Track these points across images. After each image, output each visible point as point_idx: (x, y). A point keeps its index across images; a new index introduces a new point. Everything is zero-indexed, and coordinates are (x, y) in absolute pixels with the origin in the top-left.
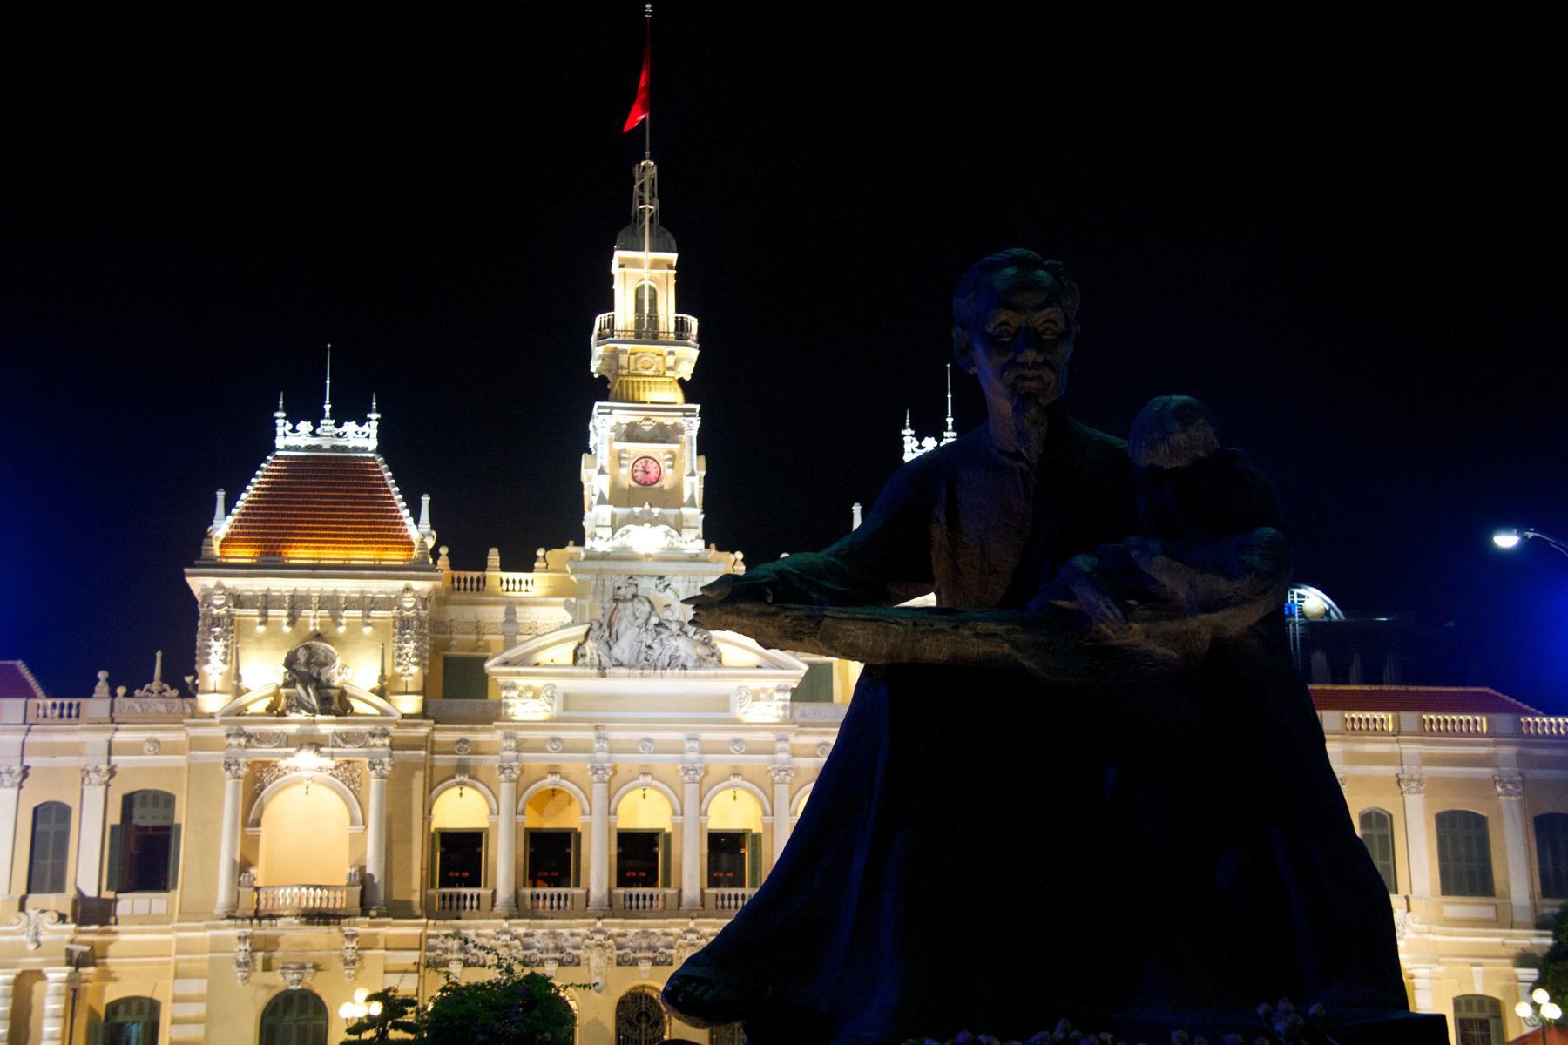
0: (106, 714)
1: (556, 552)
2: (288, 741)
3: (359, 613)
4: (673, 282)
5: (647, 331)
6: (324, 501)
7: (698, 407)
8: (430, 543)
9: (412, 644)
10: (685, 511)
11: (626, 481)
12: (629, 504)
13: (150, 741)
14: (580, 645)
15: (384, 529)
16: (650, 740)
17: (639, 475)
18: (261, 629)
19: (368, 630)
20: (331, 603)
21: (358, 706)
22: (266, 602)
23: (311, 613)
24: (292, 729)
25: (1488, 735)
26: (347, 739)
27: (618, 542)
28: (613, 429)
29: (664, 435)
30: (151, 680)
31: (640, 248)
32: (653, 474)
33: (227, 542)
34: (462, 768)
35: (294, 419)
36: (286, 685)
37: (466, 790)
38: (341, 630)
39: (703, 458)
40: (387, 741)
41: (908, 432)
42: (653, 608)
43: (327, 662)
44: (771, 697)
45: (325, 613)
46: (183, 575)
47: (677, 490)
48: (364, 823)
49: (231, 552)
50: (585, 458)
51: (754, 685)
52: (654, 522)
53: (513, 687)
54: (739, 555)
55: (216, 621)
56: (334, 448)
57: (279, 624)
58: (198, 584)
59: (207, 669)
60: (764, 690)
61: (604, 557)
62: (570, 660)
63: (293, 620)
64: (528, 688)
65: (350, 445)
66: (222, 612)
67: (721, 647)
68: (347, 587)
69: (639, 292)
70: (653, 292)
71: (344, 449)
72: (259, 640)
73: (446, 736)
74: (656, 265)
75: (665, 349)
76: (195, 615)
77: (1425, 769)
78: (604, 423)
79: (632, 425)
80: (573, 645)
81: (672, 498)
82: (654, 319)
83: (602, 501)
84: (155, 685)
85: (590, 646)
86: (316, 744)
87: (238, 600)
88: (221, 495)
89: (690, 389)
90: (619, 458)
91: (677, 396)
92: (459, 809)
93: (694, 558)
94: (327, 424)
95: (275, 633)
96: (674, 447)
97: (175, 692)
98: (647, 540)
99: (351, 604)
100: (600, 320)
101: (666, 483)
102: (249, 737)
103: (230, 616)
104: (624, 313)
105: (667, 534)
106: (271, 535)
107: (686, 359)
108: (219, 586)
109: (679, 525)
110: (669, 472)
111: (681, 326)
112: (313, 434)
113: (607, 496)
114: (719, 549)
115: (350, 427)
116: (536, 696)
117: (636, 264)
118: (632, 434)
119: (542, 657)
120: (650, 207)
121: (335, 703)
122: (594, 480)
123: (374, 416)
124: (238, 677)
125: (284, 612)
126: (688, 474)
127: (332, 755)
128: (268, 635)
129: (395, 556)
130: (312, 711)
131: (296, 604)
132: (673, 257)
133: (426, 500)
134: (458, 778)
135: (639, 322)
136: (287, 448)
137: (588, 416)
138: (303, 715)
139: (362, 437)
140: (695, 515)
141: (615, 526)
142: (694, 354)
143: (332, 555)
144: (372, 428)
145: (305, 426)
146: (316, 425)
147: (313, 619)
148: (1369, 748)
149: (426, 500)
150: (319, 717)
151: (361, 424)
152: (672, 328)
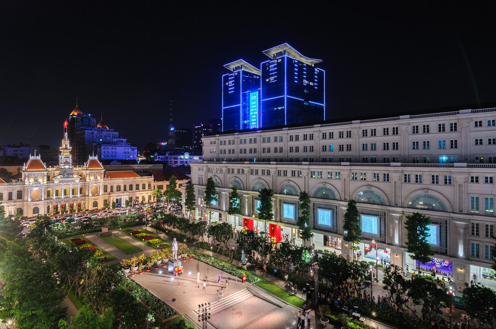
5: (66, 149)
6: (35, 164)
20: (38, 174)
22: (32, 174)
26: (40, 186)
29: (68, 157)
35: (32, 156)
47: (69, 162)
86: (37, 187)
88: (24, 163)
89: (71, 153)
91: (69, 154)
94: (35, 157)
95: (32, 177)
98: (67, 167)
106: (31, 166)
115: (37, 157)
118: (65, 157)
120: (67, 137)
126: (70, 160)
139: (39, 158)
144: (40, 157)
145: (33, 157)
147: (36, 176)
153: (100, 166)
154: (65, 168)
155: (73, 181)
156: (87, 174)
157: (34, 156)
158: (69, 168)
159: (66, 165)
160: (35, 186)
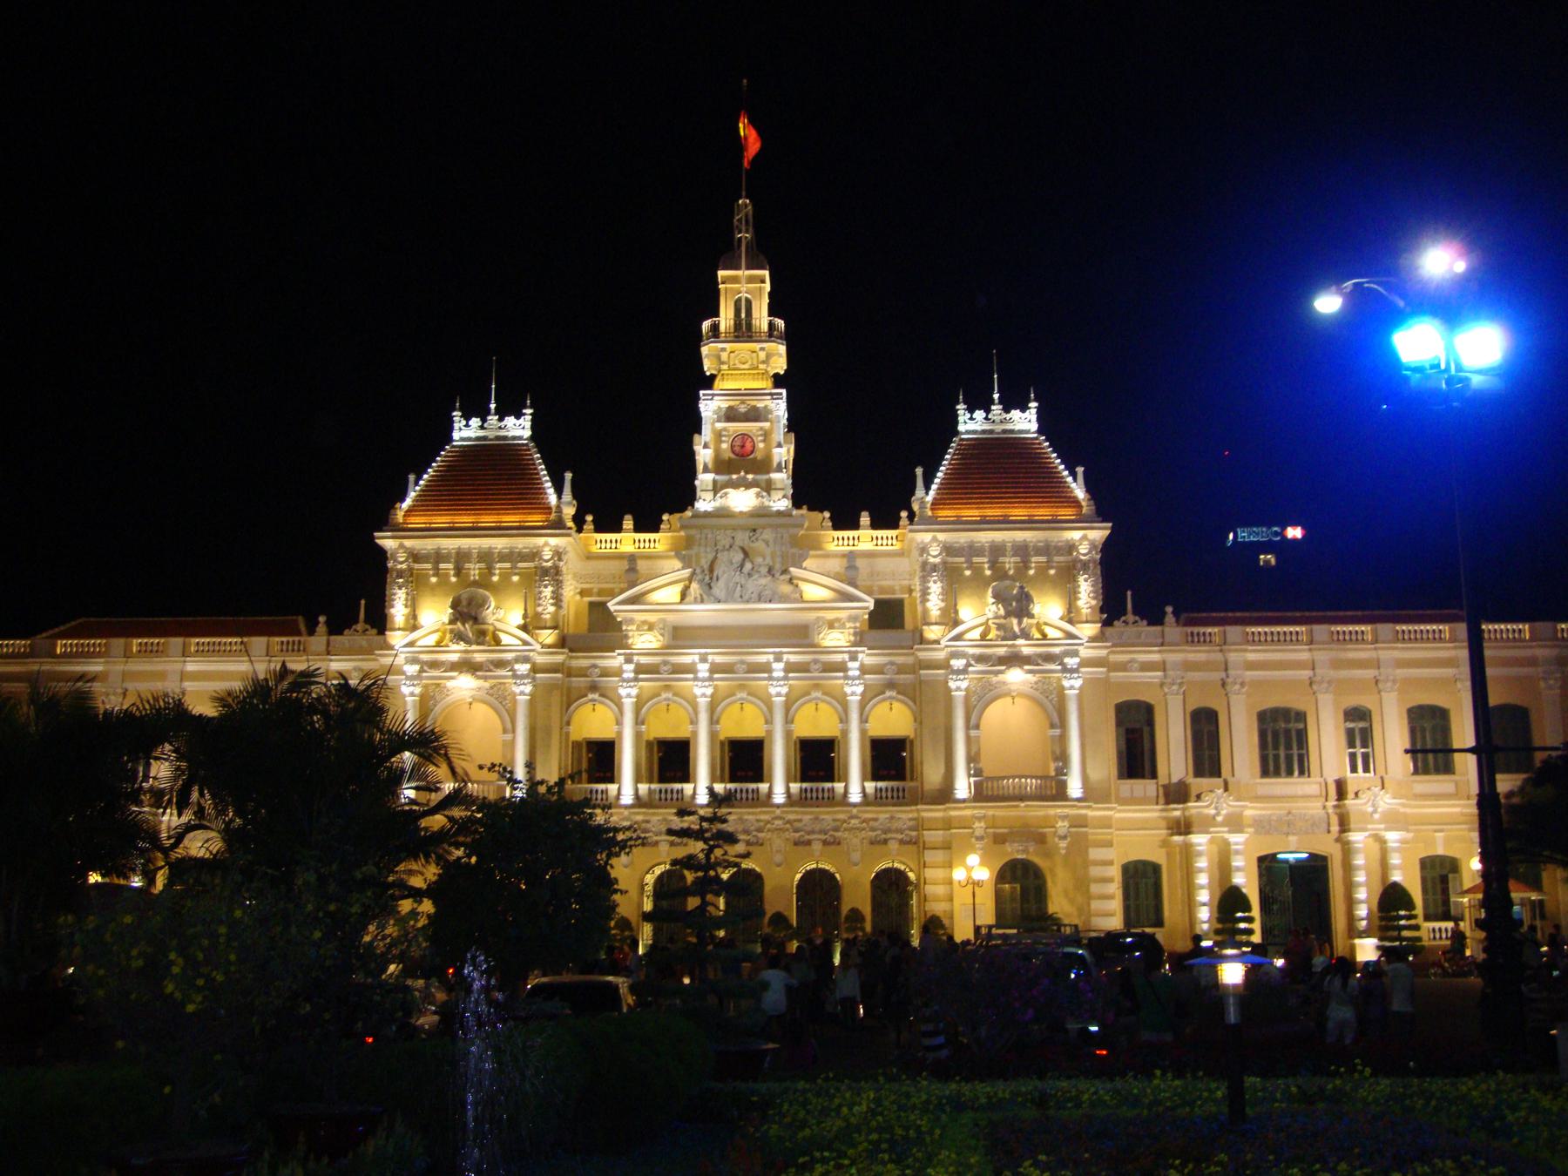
0: (324, 648)
1: (677, 515)
2: (454, 667)
3: (508, 565)
4: (766, 300)
5: (744, 331)
6: (490, 480)
7: (784, 392)
8: (569, 511)
9: (550, 589)
10: (775, 476)
11: (728, 455)
12: (730, 473)
13: (355, 669)
14: (687, 588)
15: (527, 496)
16: (742, 662)
17: (737, 449)
18: (434, 580)
19: (516, 578)
20: (487, 557)
21: (505, 639)
22: (438, 557)
23: (471, 566)
24: (455, 657)
25: (1451, 641)
27: (718, 503)
28: (715, 412)
29: (755, 415)
30: (357, 622)
31: (738, 268)
32: (748, 445)
33: (409, 512)
34: (594, 688)
35: (467, 417)
36: (451, 622)
37: (598, 707)
38: (495, 579)
39: (792, 435)
40: (528, 666)
41: (961, 407)
42: (746, 554)
43: (483, 603)
44: (843, 626)
45: (483, 565)
46: (373, 538)
48: (514, 731)
49: (412, 519)
50: (696, 437)
51: (830, 615)
52: (748, 486)
53: (631, 621)
54: (827, 514)
55: (400, 574)
56: (498, 438)
57: (447, 575)
58: (387, 542)
59: (393, 611)
60: (838, 620)
61: (706, 515)
62: (678, 599)
63: (459, 571)
64: (644, 622)
65: (510, 434)
66: (404, 566)
67: (804, 586)
68: (499, 544)
69: (737, 303)
70: (749, 302)
71: (505, 438)
72: (433, 588)
73: (582, 662)
74: (751, 280)
75: (757, 346)
76: (385, 570)
77: (1399, 671)
78: (709, 406)
79: (730, 408)
80: (679, 588)
81: (764, 466)
82: (749, 325)
83: (706, 470)
84: (360, 627)
85: (694, 586)
87: (415, 557)
90: (719, 435)
91: (766, 384)
92: (593, 722)
93: (779, 513)
96: (766, 425)
97: (375, 631)
98: (742, 500)
99: (503, 557)
100: (706, 325)
101: (759, 455)
102: (422, 663)
103: (410, 569)
104: (726, 318)
105: (758, 495)
107: (778, 358)
108: (402, 546)
109: (768, 488)
110: (761, 445)
111: (771, 326)
112: (482, 427)
113: (710, 466)
114: (810, 509)
115: (510, 421)
116: (651, 627)
117: (735, 280)
118: (731, 415)
119: (655, 597)
120: (745, 236)
121: (485, 636)
122: (704, 455)
123: (529, 411)
124: (415, 617)
125: (451, 566)
127: (485, 678)
128: (438, 584)
129: (536, 519)
130: (468, 642)
131: (461, 558)
132: (766, 273)
133: (568, 476)
134: (591, 696)
135: (738, 325)
136: (462, 439)
137: (696, 399)
138: (462, 646)
139: (519, 428)
140: (782, 478)
141: (716, 488)
142: (782, 349)
143: (488, 519)
144: (526, 421)
145: (475, 422)
146: (484, 420)
148: (1351, 655)
149: (568, 476)
150: (474, 647)
151: (518, 417)
152: (765, 327)
153: (1053, 491)
154: (722, 513)
155: (800, 635)
156: (927, 570)
157: (483, 415)
158: (761, 513)
159: (735, 485)
160: (454, 667)
